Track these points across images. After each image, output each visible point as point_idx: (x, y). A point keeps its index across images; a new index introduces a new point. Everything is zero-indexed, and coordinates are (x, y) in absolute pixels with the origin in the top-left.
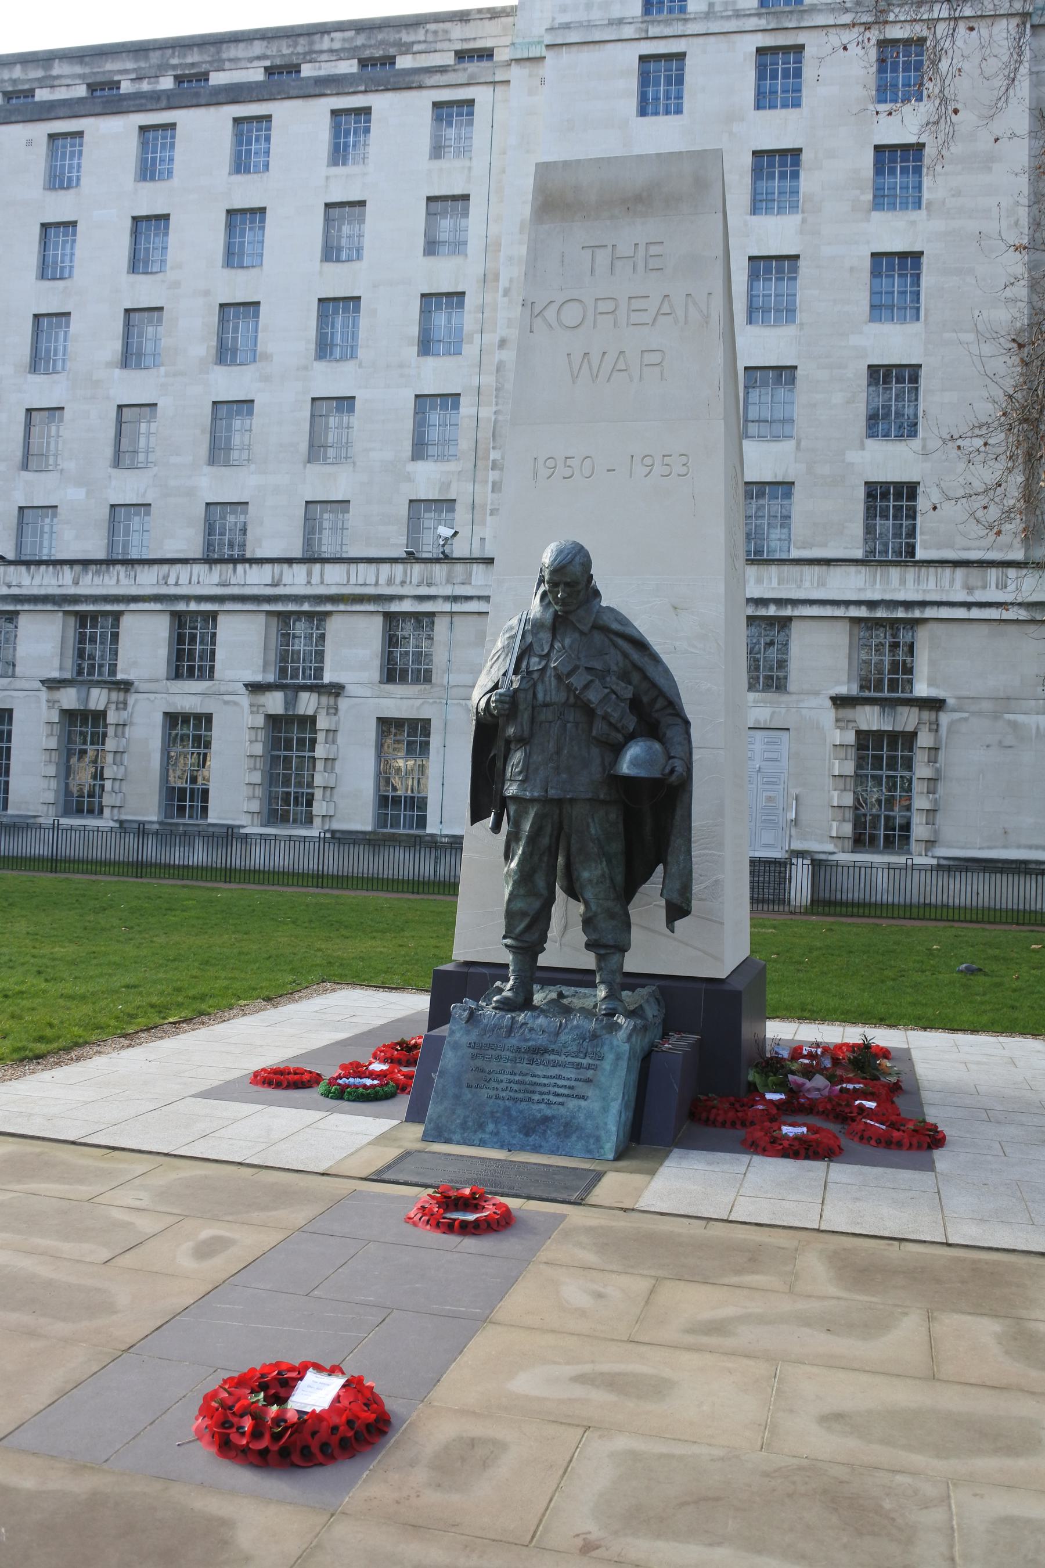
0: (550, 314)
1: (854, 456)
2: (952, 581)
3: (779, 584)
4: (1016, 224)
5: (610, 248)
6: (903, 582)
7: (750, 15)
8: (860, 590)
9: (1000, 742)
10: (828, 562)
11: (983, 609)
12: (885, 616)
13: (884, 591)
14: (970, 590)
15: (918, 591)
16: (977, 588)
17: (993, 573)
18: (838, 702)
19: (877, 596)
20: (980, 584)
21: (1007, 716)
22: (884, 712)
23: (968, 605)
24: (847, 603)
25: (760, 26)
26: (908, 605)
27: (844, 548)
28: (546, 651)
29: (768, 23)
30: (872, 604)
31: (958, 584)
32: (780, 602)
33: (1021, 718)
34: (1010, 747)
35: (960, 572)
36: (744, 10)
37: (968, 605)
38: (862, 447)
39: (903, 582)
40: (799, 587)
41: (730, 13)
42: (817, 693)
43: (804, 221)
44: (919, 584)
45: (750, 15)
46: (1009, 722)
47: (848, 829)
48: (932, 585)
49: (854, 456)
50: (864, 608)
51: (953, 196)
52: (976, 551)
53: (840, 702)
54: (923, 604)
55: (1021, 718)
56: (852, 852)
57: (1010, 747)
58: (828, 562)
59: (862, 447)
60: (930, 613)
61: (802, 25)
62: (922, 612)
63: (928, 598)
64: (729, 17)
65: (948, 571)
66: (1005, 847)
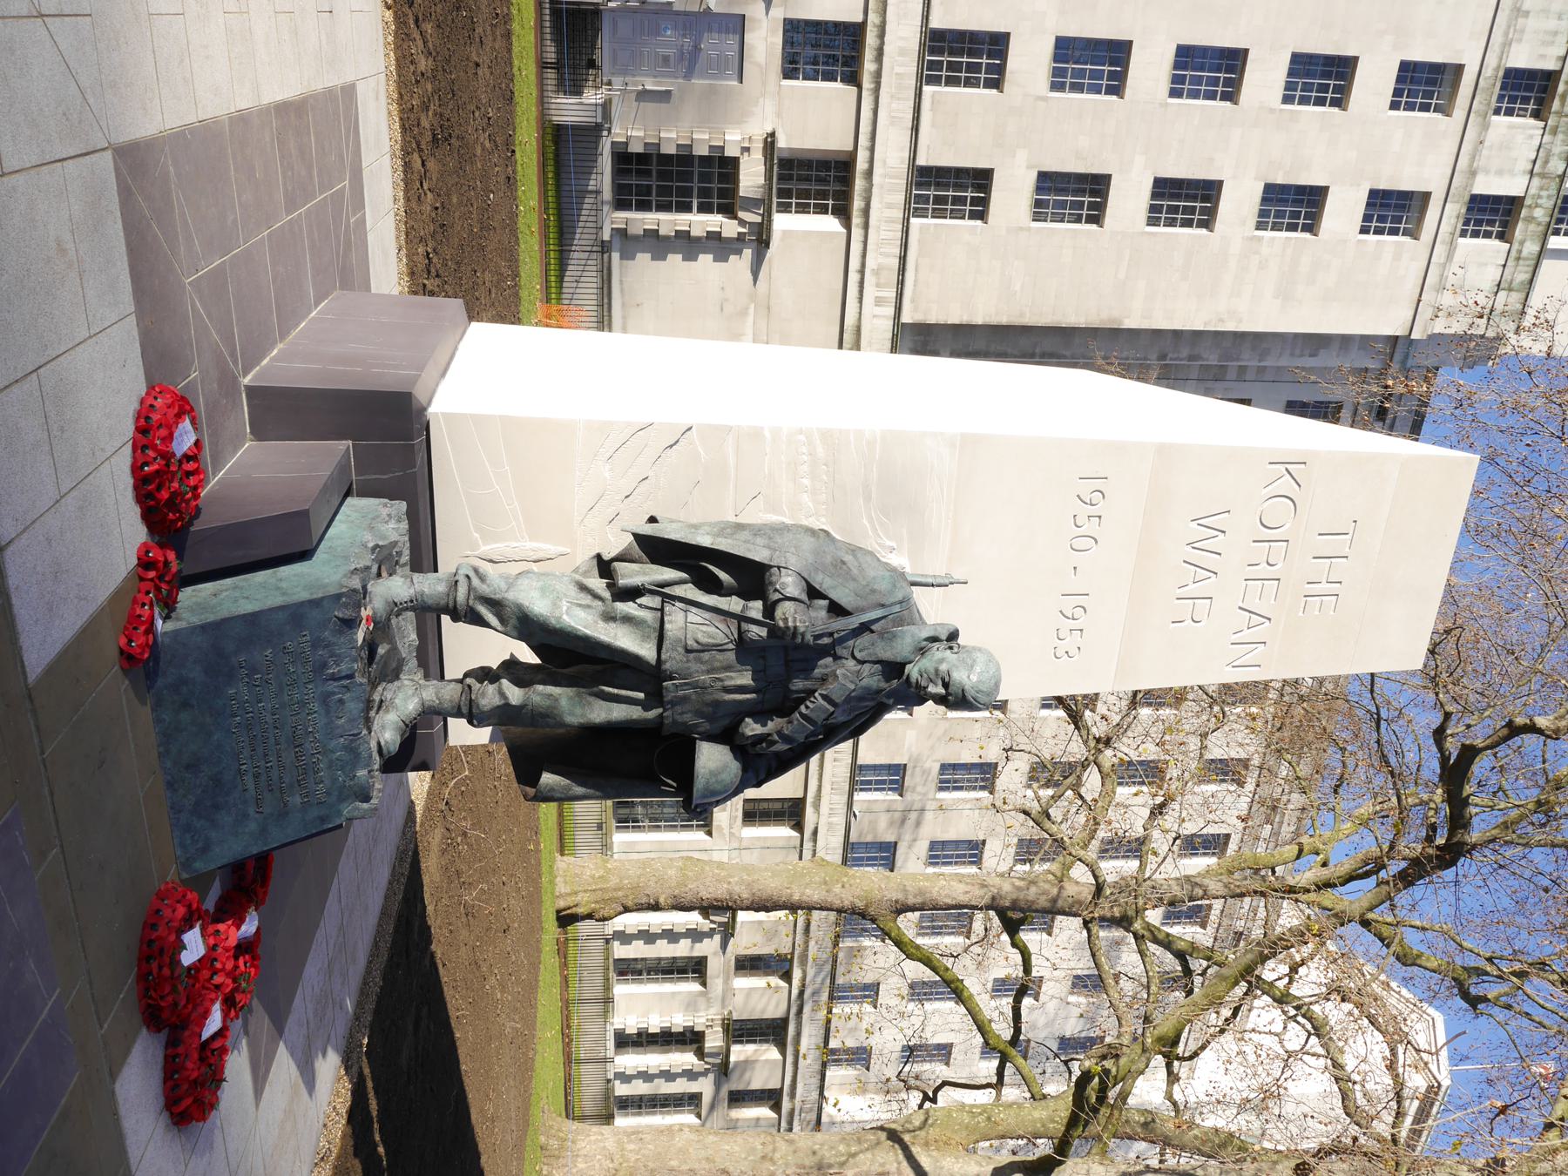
0: (1286, 485)
1: (1022, 156)
2: (887, 255)
3: (897, 74)
4: (1221, 320)
5: (1346, 551)
6: (890, 206)
7: (1501, 59)
8: (885, 162)
9: (726, 300)
10: (916, 129)
11: (857, 285)
12: (857, 188)
13: (882, 187)
14: (876, 272)
15: (879, 221)
16: (879, 279)
17: (891, 294)
18: (769, 140)
19: (876, 179)
20: (882, 281)
21: (753, 306)
22: (758, 187)
23: (862, 272)
24: (872, 150)
25: (1486, 69)
26: (866, 212)
27: (928, 146)
28: (857, 654)
29: (1485, 79)
30: (869, 173)
31: (881, 260)
32: (878, 75)
33: (750, 319)
34: (722, 310)
35: (894, 263)
36: (1508, 52)
37: (862, 272)
38: (1029, 167)
39: (890, 206)
40: (892, 97)
41: (1510, 36)
42: (779, 115)
43: (1272, 111)
44: (886, 222)
45: (1501, 59)
46: (747, 309)
47: (636, 148)
48: (884, 235)
49: (1022, 156)
50: (866, 166)
51: (1260, 262)
52: (913, 278)
53: (770, 143)
54: (866, 226)
55: (750, 319)
56: (612, 152)
57: (722, 310)
58: (916, 129)
59: (1029, 167)
60: (857, 233)
61: (1472, 115)
62: (857, 225)
63: (871, 231)
64: (1506, 34)
65: (897, 251)
66: (623, 305)
